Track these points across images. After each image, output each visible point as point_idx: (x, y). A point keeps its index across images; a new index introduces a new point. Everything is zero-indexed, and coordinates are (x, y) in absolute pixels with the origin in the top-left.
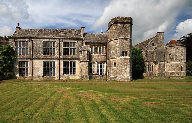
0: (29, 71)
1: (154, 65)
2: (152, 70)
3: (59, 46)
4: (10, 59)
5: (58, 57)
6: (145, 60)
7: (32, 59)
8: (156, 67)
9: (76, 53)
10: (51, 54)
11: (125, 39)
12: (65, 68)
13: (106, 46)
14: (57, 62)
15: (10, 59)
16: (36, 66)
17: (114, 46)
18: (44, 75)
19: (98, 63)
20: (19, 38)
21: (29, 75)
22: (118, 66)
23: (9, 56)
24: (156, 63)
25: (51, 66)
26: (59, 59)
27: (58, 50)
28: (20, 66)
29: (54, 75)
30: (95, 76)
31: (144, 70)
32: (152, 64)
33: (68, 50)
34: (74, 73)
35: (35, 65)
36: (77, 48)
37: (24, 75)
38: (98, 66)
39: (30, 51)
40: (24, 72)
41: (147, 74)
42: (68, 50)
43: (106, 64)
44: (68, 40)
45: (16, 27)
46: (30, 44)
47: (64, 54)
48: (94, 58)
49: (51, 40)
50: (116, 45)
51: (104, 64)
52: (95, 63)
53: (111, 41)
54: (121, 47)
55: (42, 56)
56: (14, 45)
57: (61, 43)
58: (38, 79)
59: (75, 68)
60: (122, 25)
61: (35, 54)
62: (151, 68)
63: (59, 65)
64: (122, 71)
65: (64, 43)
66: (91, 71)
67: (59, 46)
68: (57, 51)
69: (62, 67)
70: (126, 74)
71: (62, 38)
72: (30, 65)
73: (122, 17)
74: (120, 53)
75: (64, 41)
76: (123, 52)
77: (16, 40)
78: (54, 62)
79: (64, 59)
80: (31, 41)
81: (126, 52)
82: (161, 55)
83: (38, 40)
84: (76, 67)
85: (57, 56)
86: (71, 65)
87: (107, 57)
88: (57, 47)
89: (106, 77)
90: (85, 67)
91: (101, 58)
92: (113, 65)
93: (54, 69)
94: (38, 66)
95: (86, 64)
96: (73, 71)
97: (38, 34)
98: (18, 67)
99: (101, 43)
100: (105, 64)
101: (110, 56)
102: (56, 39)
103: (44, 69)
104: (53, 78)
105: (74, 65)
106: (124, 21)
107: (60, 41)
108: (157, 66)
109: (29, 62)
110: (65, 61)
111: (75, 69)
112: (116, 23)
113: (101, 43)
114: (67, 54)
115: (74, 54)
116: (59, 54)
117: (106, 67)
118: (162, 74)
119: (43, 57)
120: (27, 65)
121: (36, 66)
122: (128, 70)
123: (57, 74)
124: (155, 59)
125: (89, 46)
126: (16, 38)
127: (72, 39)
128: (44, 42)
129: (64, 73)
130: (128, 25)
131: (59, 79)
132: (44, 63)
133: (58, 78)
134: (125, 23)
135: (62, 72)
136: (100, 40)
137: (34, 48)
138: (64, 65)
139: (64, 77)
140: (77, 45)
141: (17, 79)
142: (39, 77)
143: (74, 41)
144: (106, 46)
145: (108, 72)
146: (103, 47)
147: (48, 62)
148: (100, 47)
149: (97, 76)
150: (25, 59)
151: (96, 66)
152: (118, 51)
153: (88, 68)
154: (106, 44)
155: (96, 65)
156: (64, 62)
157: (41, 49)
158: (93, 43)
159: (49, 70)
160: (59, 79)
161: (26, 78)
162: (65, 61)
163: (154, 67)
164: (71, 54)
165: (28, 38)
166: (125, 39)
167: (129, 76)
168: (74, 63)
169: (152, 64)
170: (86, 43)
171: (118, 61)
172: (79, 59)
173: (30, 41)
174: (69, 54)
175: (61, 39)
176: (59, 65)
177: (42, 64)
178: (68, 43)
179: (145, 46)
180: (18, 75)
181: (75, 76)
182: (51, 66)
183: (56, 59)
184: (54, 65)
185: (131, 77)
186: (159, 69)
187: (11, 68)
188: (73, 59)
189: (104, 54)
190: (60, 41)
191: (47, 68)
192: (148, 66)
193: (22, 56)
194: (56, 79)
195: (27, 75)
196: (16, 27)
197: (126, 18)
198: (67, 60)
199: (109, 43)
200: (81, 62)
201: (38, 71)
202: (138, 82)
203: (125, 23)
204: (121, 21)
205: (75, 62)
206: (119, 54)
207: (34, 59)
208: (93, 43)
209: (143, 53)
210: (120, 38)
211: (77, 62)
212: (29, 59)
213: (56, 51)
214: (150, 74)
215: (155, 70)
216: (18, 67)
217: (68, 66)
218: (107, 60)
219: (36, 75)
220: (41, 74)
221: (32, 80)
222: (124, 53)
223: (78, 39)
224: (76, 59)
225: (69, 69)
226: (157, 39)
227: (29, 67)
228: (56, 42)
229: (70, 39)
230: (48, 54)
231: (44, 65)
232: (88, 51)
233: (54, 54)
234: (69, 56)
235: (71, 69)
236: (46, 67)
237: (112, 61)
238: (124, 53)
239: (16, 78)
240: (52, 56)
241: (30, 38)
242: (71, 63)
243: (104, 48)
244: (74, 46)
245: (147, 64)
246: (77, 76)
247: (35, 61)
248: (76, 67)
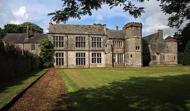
0: (65, 61)
1: (157, 55)
2: (156, 60)
3: (88, 40)
4: (50, 51)
5: (88, 49)
6: (151, 51)
7: (67, 51)
8: (158, 57)
9: (102, 46)
10: (82, 46)
11: (138, 38)
12: (93, 58)
13: (124, 41)
14: (87, 53)
15: (50, 51)
16: (70, 57)
17: (131, 42)
18: (77, 64)
19: (118, 55)
20: (57, 34)
21: (64, 64)
22: (134, 57)
23: (49, 48)
24: (158, 54)
25: (60, 56)
26: (89, 51)
27: (88, 44)
28: (57, 56)
29: (85, 64)
30: (116, 64)
31: (150, 60)
32: (155, 54)
33: (96, 43)
34: (101, 62)
35: (68, 56)
36: (103, 42)
37: (60, 64)
38: (118, 56)
39: (65, 44)
40: (61, 62)
41: (152, 63)
42: (96, 43)
43: (124, 55)
44: (96, 36)
45: (50, 23)
46: (65, 38)
47: (93, 47)
48: (115, 50)
49: (82, 36)
50: (132, 42)
51: (122, 55)
52: (116, 54)
53: (128, 38)
54: (135, 44)
55: (75, 48)
56: (52, 39)
57: (90, 38)
58: (72, 67)
59: (85, 58)
60: (136, 28)
61: (69, 46)
62: (154, 58)
63: (88, 56)
64: (135, 60)
65: (93, 38)
66: (113, 60)
67: (88, 40)
68: (87, 44)
69: (91, 57)
70: (139, 63)
71: (91, 35)
72: (65, 55)
73: (136, 23)
74: (135, 47)
75: (92, 36)
76: (137, 47)
77: (54, 35)
78: (85, 54)
79: (93, 51)
80: (66, 36)
81: (139, 47)
82: (162, 48)
83: (72, 35)
84: (102, 57)
85: (87, 48)
86: (98, 56)
87: (125, 49)
88: (87, 41)
89: (124, 65)
90: (110, 57)
91: (120, 51)
92: (130, 56)
93: (85, 59)
94: (71, 57)
95: (110, 55)
96: (99, 61)
97: (70, 30)
98: (55, 57)
99: (120, 39)
100: (123, 55)
101: (127, 50)
102: (86, 34)
103: (77, 59)
104: (84, 66)
105: (100, 56)
106: (137, 25)
107: (89, 36)
108: (159, 56)
109: (65, 53)
110: (93, 52)
111: (101, 59)
112: (132, 26)
113: (120, 39)
114: (95, 46)
115: (100, 47)
116: (88, 46)
117: (124, 57)
118: (163, 62)
119: (75, 49)
120: (63, 56)
121: (70, 57)
122: (140, 60)
123: (87, 63)
124: (157, 51)
125: (112, 40)
126: (54, 34)
127: (99, 35)
128: (77, 37)
129: (93, 62)
130: (139, 28)
131: (89, 67)
132: (77, 54)
133: (88, 67)
134: (137, 27)
135: (91, 61)
136: (119, 37)
137: (68, 42)
138: (93, 56)
139: (93, 65)
140: (102, 39)
141: (54, 67)
142: (73, 65)
143: (100, 36)
144: (124, 41)
145: (126, 61)
146: (122, 42)
147: (80, 54)
148: (120, 42)
149: (117, 64)
150: (61, 51)
151: (116, 56)
152: (134, 46)
153: (112, 58)
154: (124, 40)
155: (117, 56)
156: (93, 54)
157: (74, 43)
158: (114, 39)
159: (80, 60)
160: (89, 67)
161: (62, 67)
162: (93, 52)
163: (157, 57)
164: (98, 47)
165: (64, 34)
166: (138, 38)
167: (141, 64)
168: (101, 54)
169: (155, 54)
170: (109, 39)
171: (133, 53)
172: (104, 51)
173: (65, 36)
174: (96, 47)
175: (90, 35)
176: (88, 56)
177: (75, 55)
178: (95, 38)
179: (150, 40)
180: (55, 64)
181: (101, 64)
182: (60, 56)
183: (86, 51)
184: (84, 56)
185: (142, 65)
186: (161, 58)
187: (50, 58)
188: (100, 51)
189: (122, 47)
190: (89, 36)
191: (82, 58)
192: (153, 56)
193: (58, 48)
194: (87, 67)
195: (63, 64)
196: (50, 23)
197: (138, 23)
198: (95, 52)
199: (127, 40)
200: (106, 53)
201: (72, 61)
202: (146, 68)
203: (137, 27)
204: (135, 25)
205: (101, 53)
206: (134, 48)
207: (69, 51)
208: (114, 39)
209: (149, 46)
210: (135, 37)
211: (103, 53)
212: (64, 51)
213: (86, 45)
214: (154, 62)
215: (158, 60)
216: (55, 57)
217: (95, 56)
218: (124, 53)
219: (70, 64)
220: (75, 63)
221: (67, 68)
222: (137, 48)
223: (104, 35)
224: (102, 51)
225: (97, 59)
226: (159, 35)
227: (65, 57)
228: (86, 37)
229: (97, 35)
230: (79, 47)
231: (77, 56)
232: (111, 45)
233: (84, 46)
234: (97, 49)
235: (98, 59)
236: (94, 57)
237: (130, 53)
238: (137, 48)
239: (53, 66)
240: (83, 48)
241: (66, 34)
242: (98, 54)
243: (123, 43)
244: (100, 40)
245: (152, 54)
246: (103, 64)
247: (69, 53)
248: (102, 57)
